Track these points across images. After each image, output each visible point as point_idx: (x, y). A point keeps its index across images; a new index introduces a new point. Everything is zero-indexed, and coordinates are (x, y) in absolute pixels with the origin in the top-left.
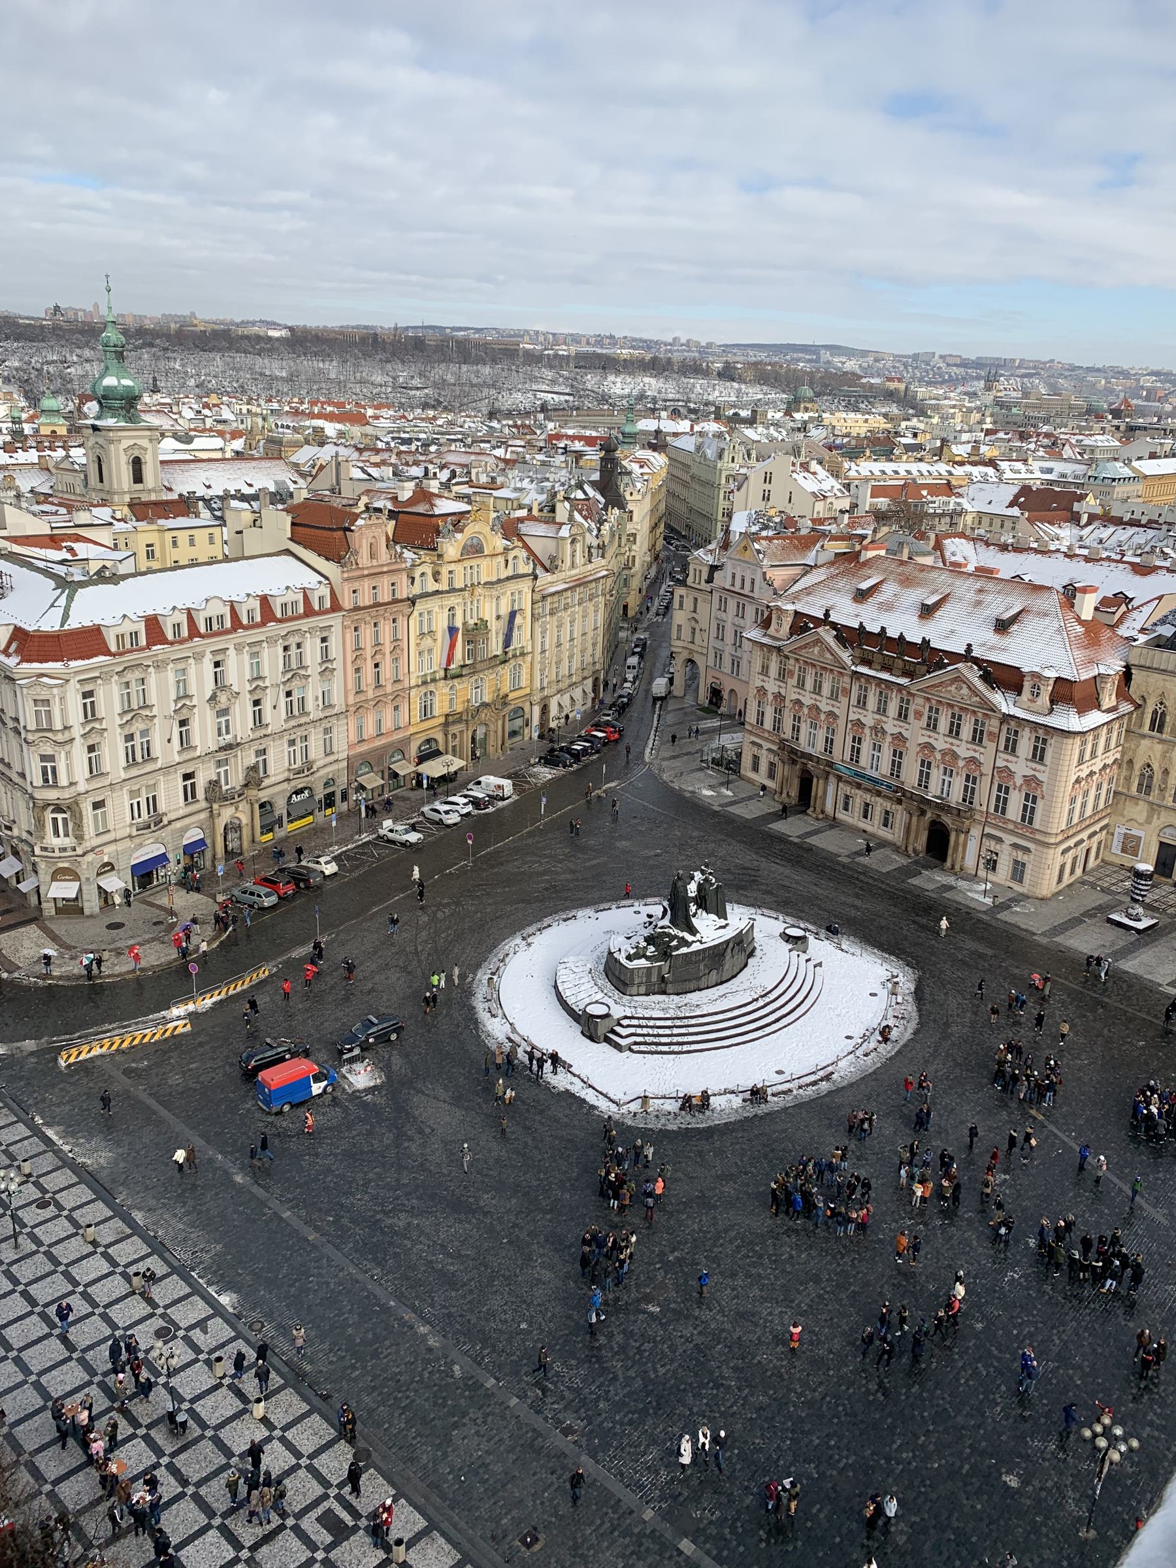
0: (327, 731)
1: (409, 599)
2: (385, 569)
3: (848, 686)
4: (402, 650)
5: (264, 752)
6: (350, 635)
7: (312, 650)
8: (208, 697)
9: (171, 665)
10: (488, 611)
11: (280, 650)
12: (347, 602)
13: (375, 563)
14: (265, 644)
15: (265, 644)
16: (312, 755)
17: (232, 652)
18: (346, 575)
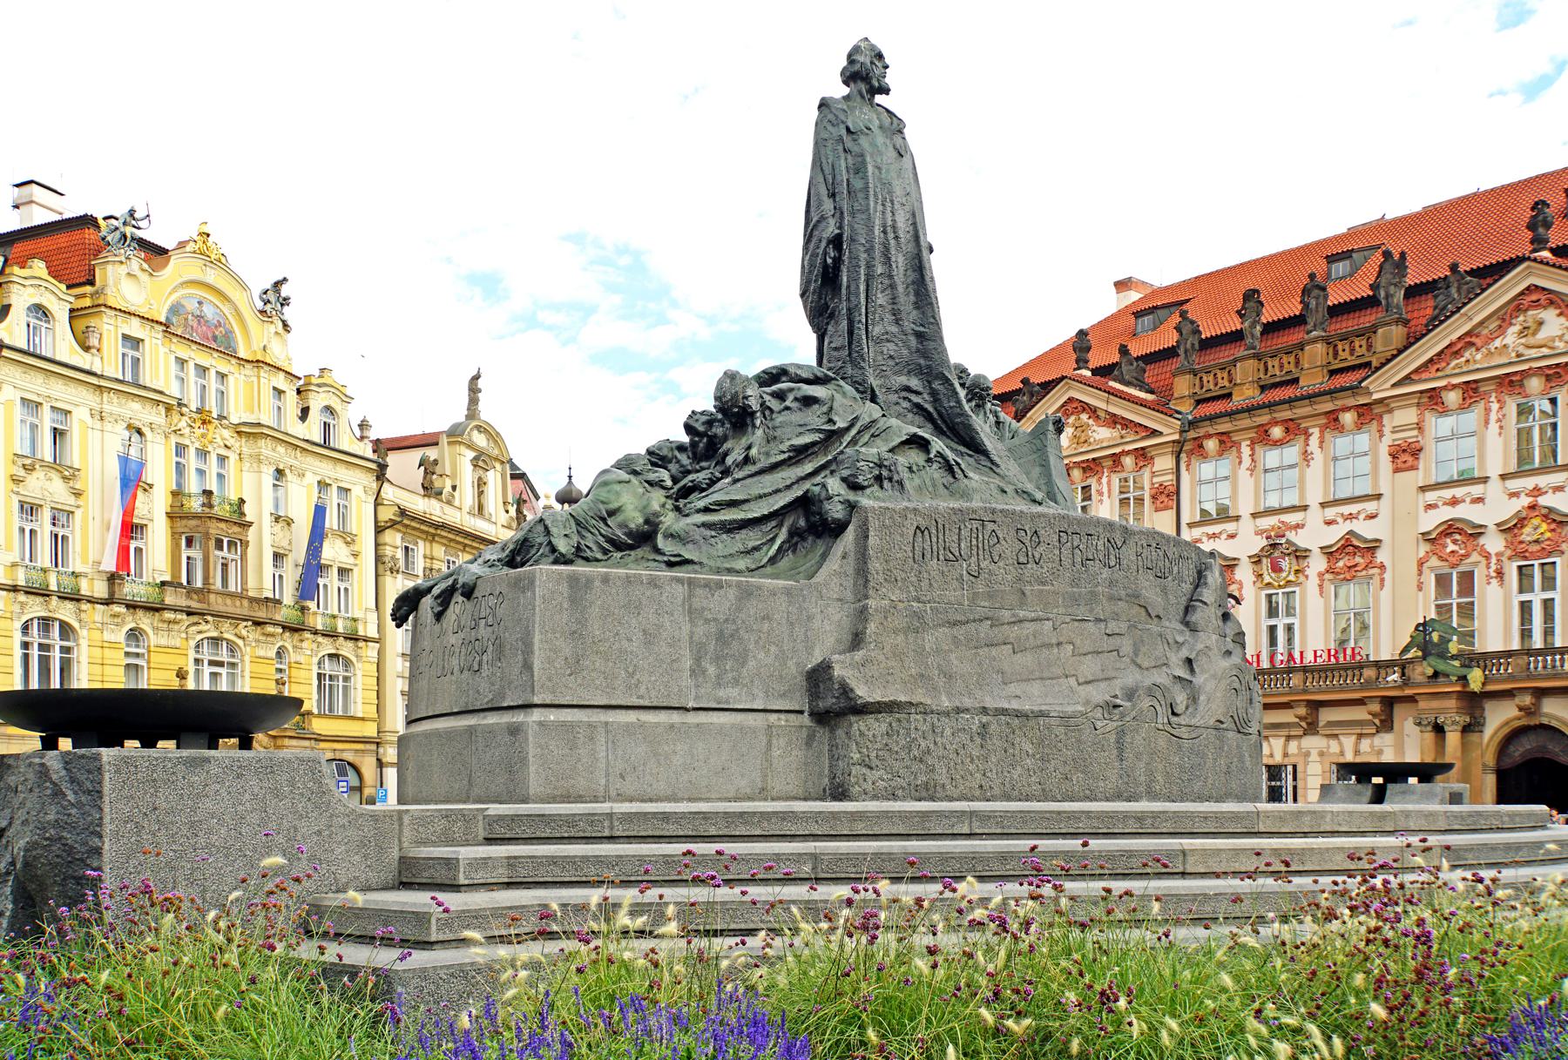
3: (1169, 479)
10: (247, 483)
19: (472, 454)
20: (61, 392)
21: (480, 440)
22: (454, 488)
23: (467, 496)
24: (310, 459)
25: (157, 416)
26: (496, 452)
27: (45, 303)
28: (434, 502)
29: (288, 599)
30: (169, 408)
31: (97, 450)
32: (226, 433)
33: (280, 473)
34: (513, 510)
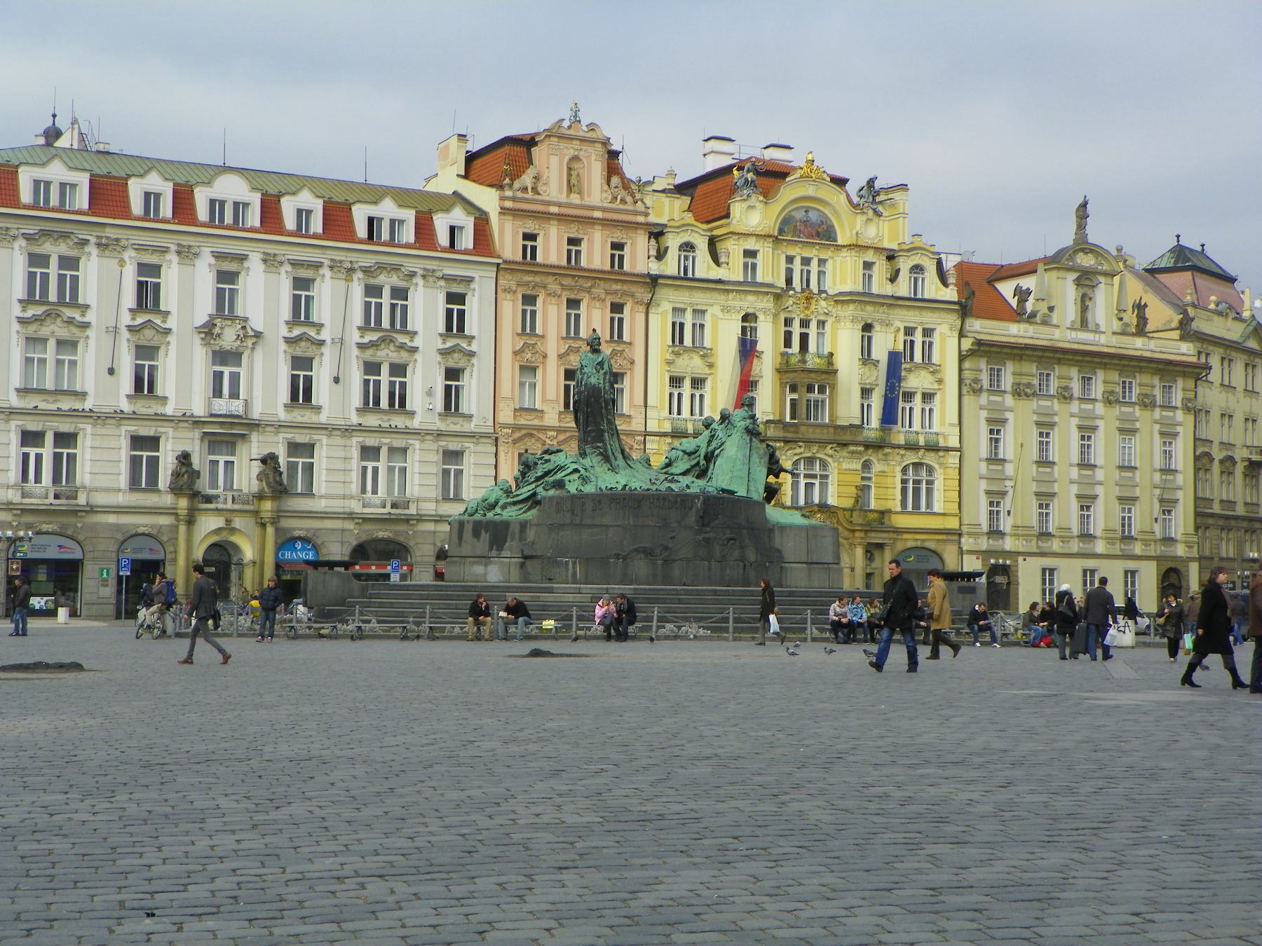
0: (453, 456)
1: (649, 275)
2: (598, 214)
4: (632, 363)
5: (309, 449)
6: (511, 309)
7: (426, 308)
8: (198, 324)
9: (129, 255)
11: (357, 290)
12: (508, 242)
13: (575, 198)
14: (325, 271)
15: (325, 271)
16: (413, 490)
17: (255, 263)
18: (509, 204)
19: (1075, 275)
20: (700, 299)
21: (1086, 261)
22: (1051, 309)
23: (1068, 311)
24: (898, 311)
25: (767, 303)
26: (1106, 267)
27: (692, 240)
28: (1023, 326)
29: (875, 422)
30: (778, 297)
31: (723, 335)
32: (823, 303)
33: (867, 328)
34: (1131, 318)
